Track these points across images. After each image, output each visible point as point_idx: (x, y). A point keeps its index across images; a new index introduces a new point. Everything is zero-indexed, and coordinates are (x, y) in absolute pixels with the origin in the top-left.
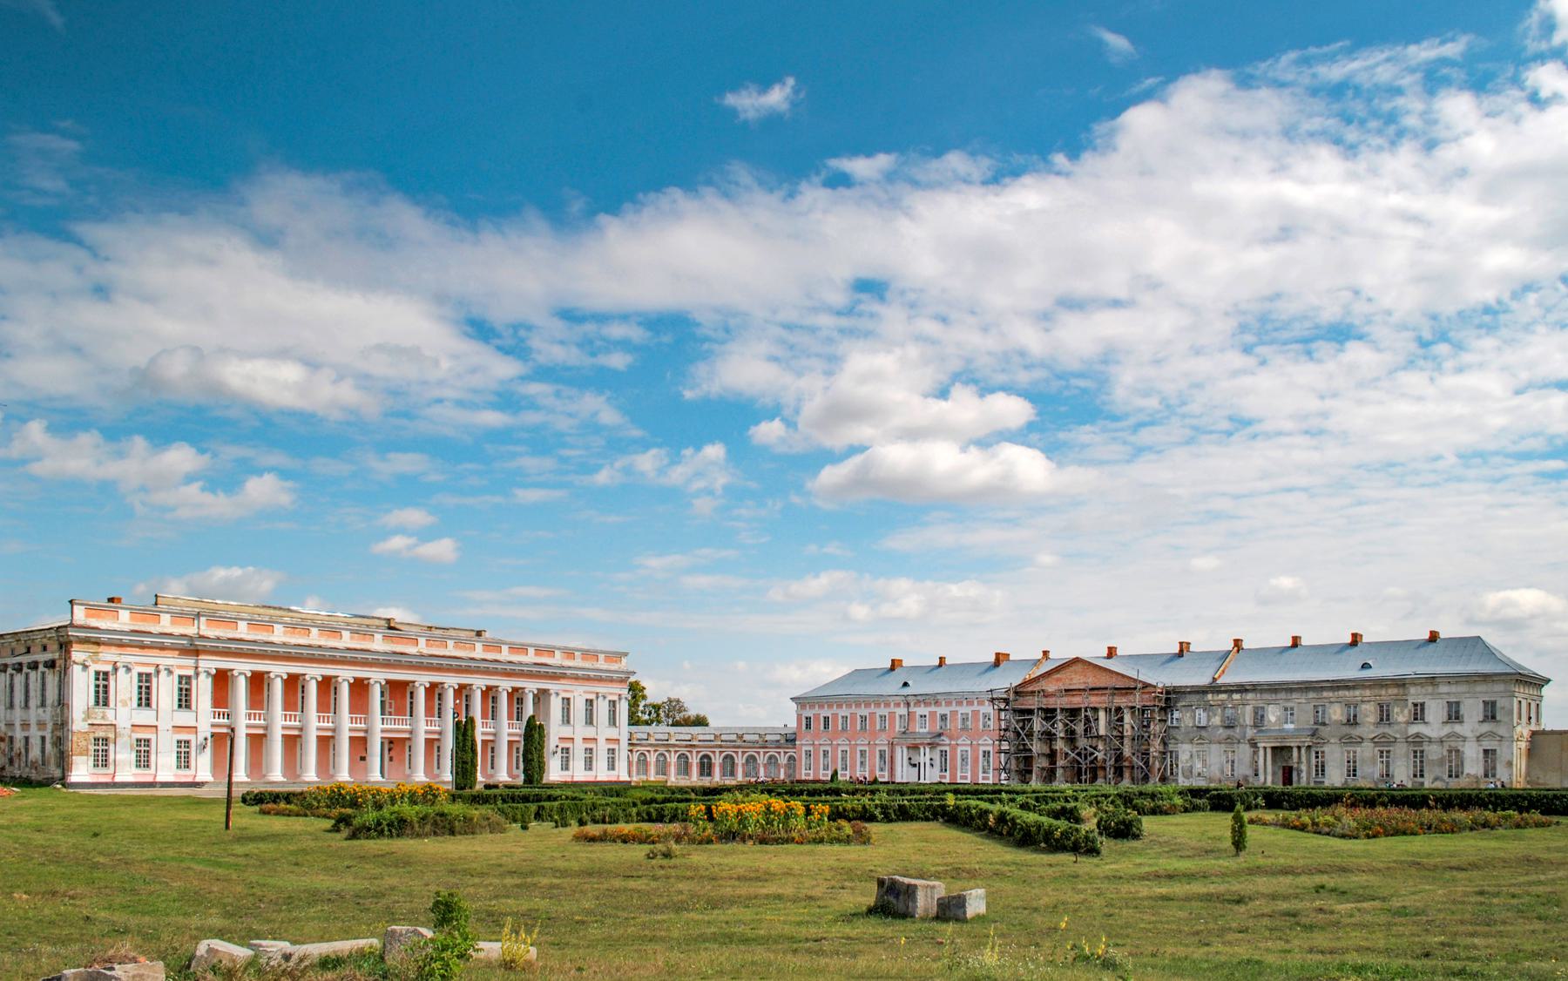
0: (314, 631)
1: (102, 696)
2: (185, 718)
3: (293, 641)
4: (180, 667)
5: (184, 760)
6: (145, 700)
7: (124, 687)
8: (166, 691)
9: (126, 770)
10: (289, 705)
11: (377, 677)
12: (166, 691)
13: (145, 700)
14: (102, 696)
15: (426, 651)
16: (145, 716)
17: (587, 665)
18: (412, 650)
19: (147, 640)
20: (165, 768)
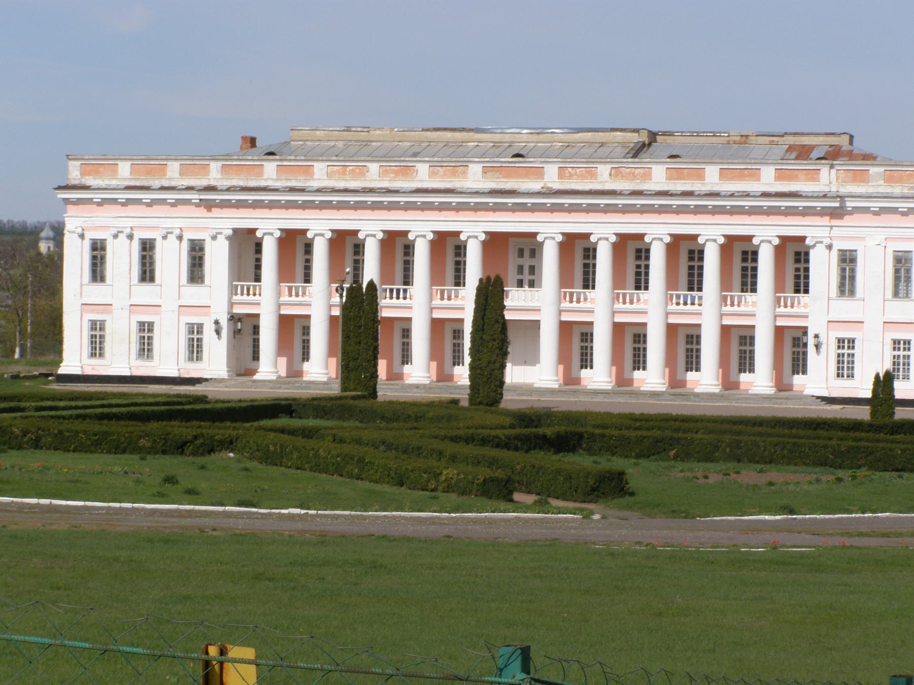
0: (374, 167)
1: (97, 272)
2: (194, 294)
3: (341, 185)
4: (190, 229)
5: (195, 349)
6: (147, 274)
7: (122, 260)
8: (171, 260)
9: (120, 361)
10: (285, 273)
11: (474, 229)
12: (171, 260)
13: (147, 274)
14: (97, 272)
15: (557, 186)
16: (145, 293)
17: (897, 190)
18: (536, 186)
19: (146, 196)
20: (168, 361)
